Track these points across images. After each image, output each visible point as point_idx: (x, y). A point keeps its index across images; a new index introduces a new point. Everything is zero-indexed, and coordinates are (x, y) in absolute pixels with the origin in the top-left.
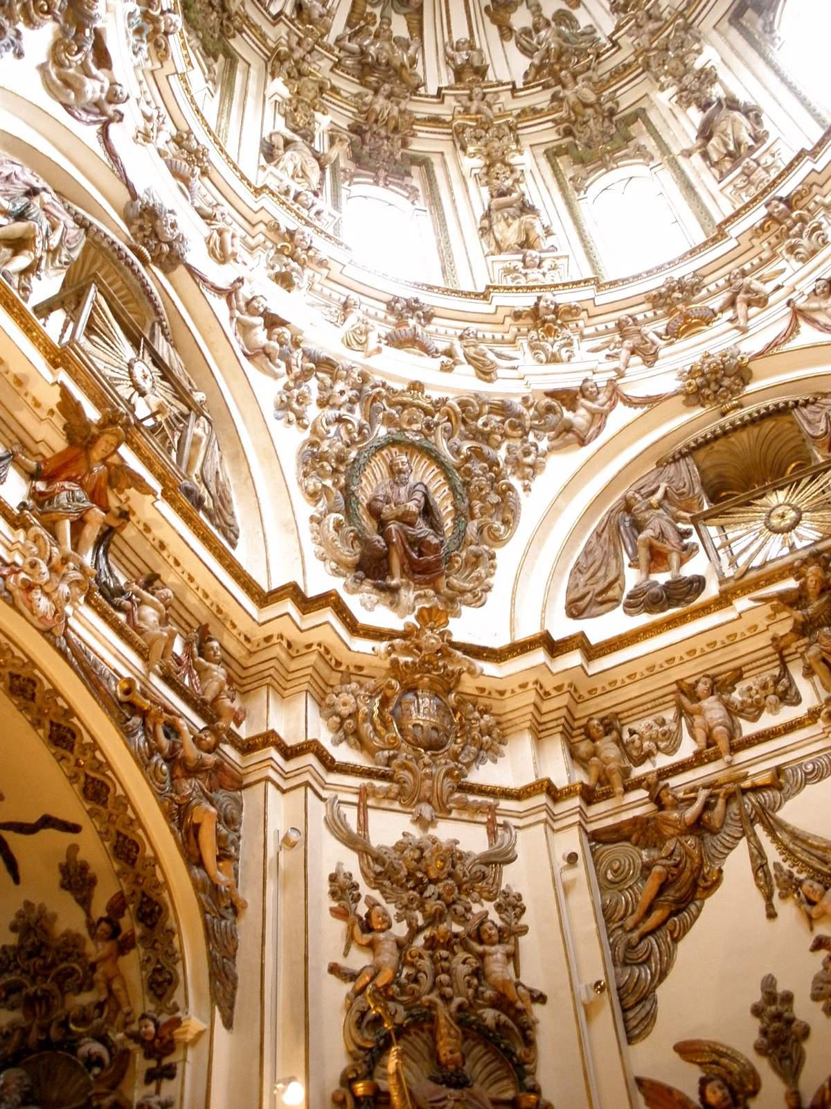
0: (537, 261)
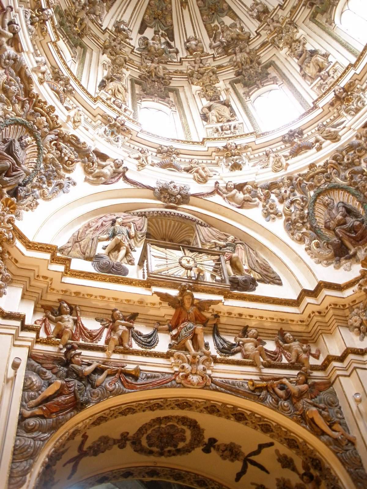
0: (326, 74)
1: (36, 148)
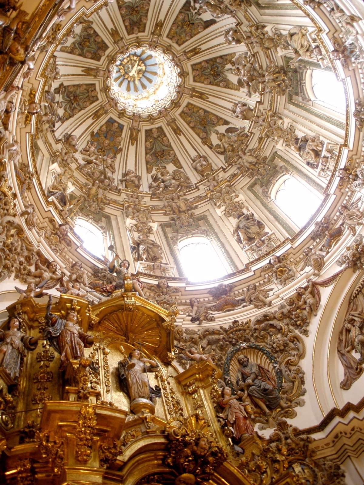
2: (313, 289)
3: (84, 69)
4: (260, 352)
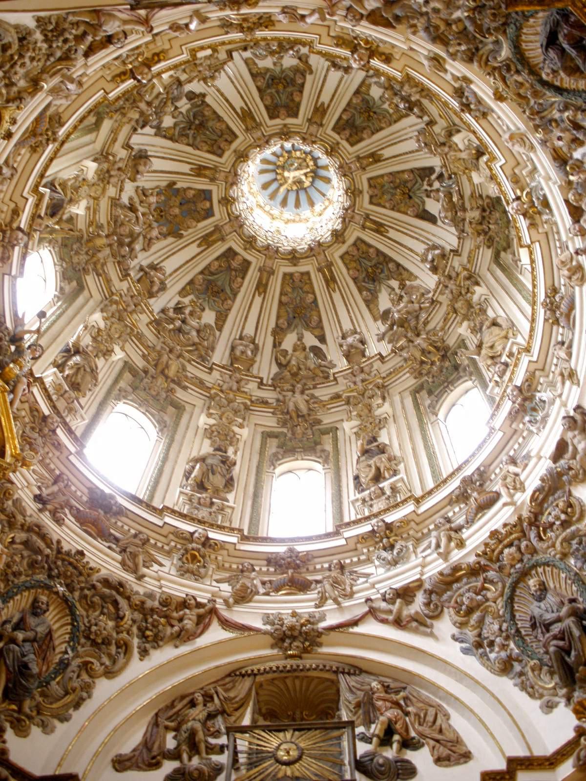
1: (547, 569)
2: (207, 615)
3: (246, 108)
4: (69, 618)
